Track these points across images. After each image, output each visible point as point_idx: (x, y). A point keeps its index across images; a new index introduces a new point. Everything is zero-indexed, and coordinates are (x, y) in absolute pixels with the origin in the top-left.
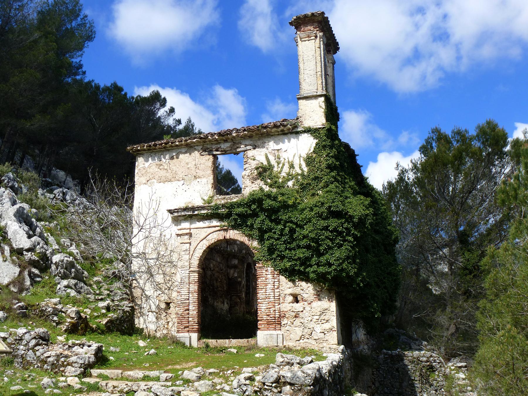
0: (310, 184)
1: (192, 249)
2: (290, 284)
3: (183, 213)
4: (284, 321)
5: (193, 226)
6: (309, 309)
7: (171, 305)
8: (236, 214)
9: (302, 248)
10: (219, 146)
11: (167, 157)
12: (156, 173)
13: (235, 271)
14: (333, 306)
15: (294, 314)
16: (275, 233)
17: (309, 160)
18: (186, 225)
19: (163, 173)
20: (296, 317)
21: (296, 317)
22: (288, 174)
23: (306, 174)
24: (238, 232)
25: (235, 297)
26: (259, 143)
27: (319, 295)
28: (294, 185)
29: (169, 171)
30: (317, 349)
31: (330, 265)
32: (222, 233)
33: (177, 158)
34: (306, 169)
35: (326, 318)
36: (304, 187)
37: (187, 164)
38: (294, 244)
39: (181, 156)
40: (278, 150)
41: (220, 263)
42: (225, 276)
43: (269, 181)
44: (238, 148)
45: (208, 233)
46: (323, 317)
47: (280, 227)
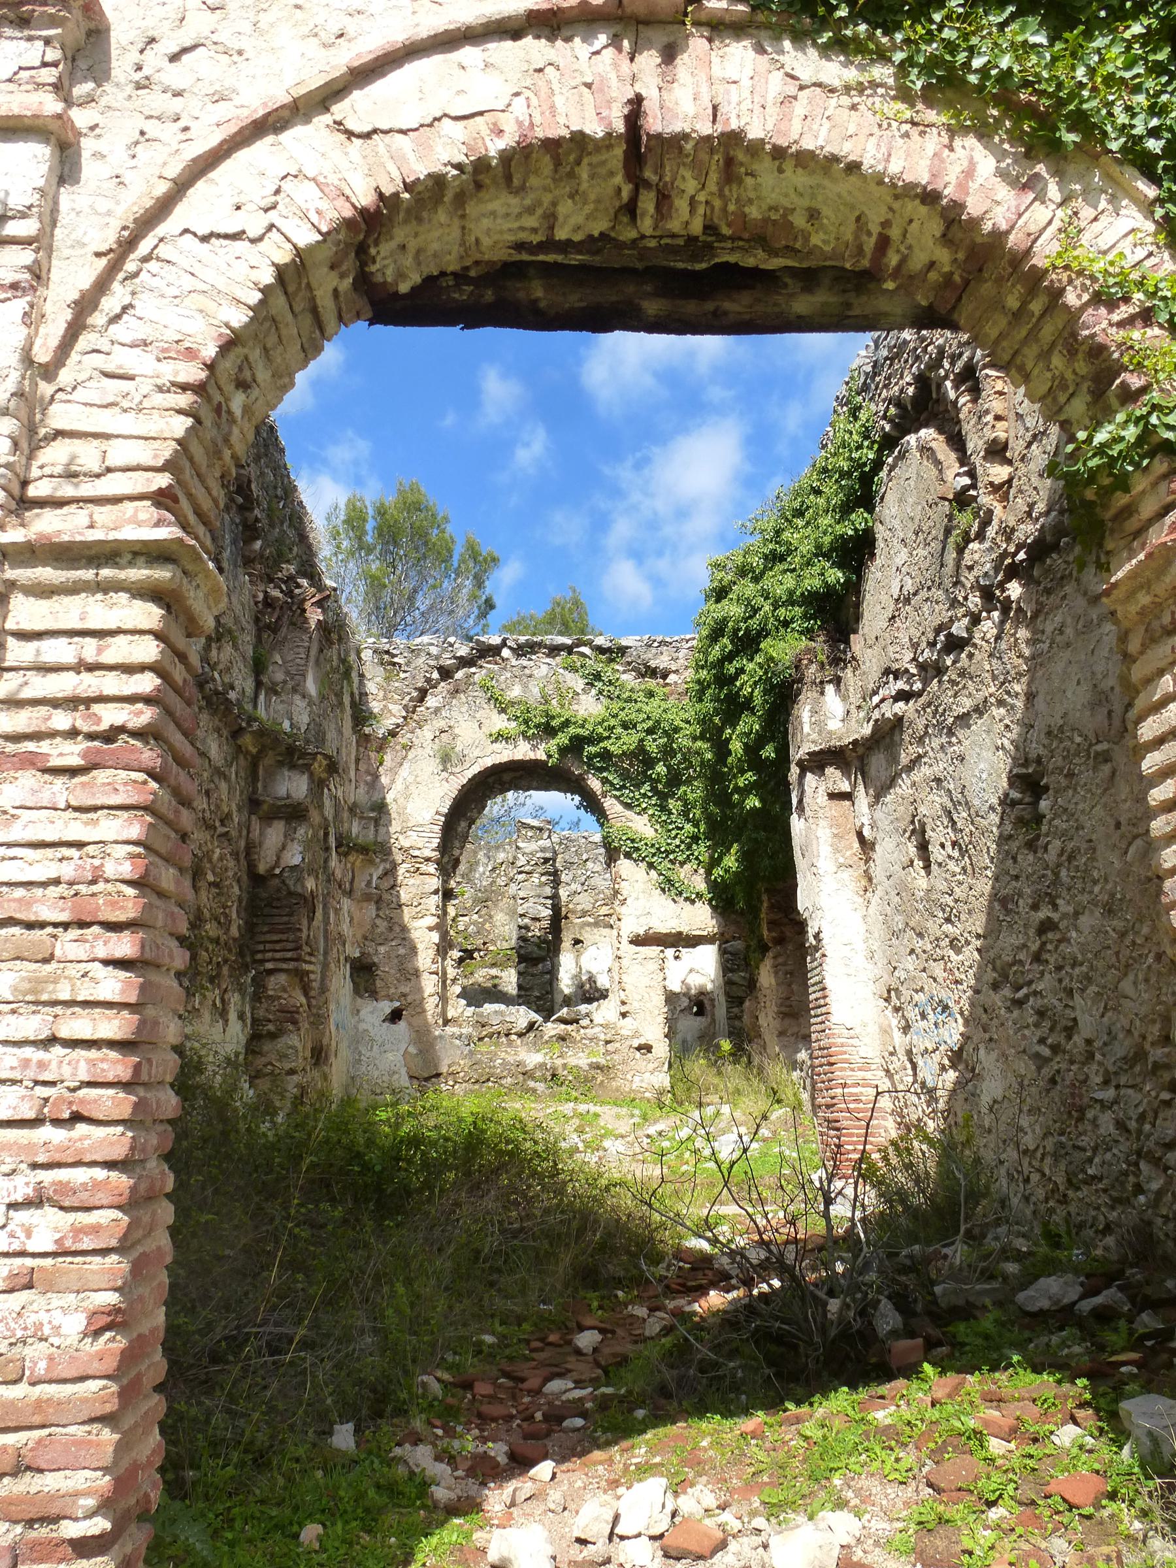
13: (289, 836)
24: (835, 71)
25: (282, 978)
41: (219, 773)
42: (235, 855)
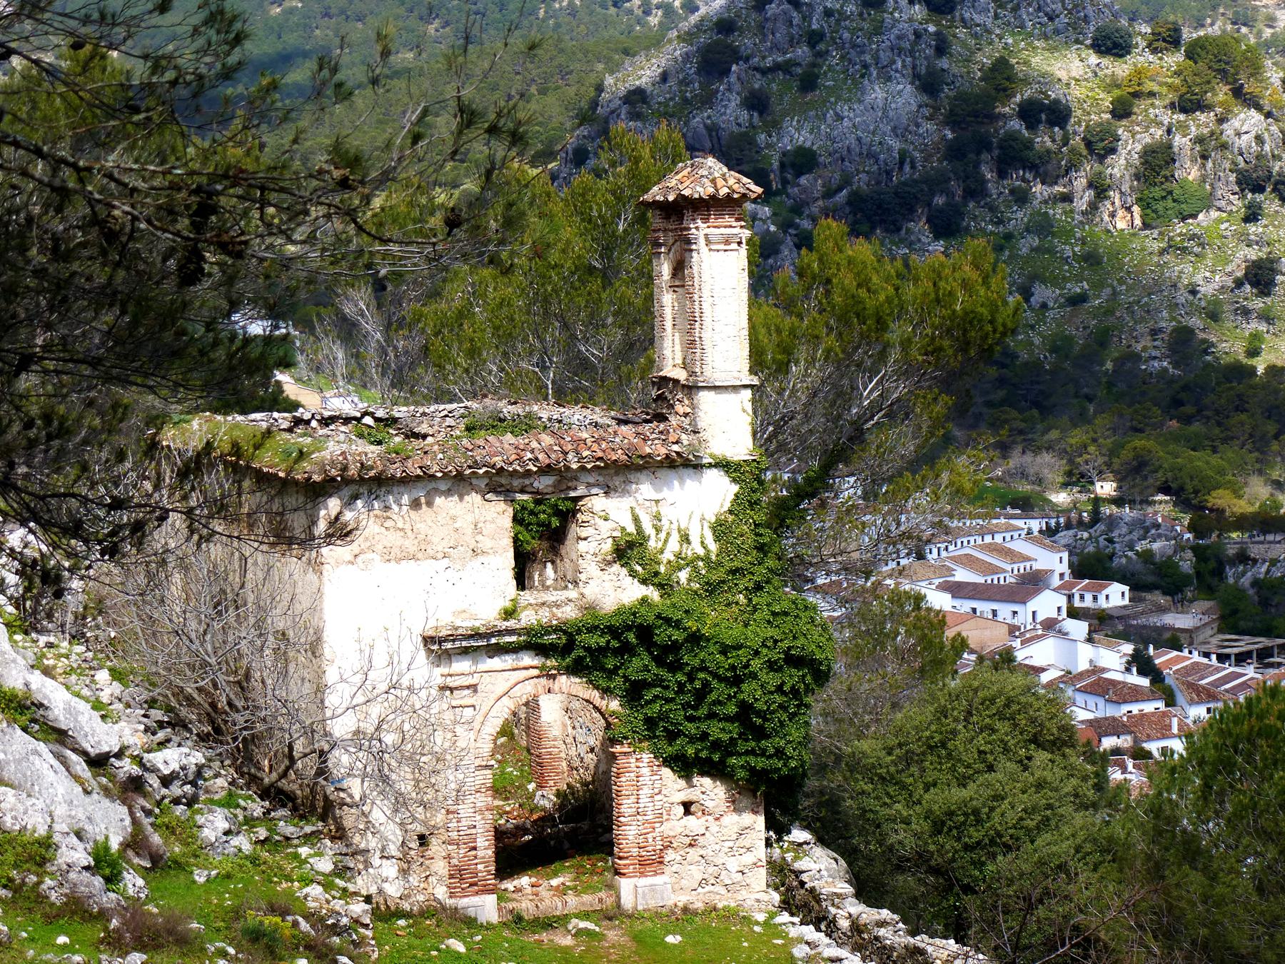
0: (723, 582)
1: (479, 719)
2: (682, 783)
3: (464, 644)
4: (670, 855)
5: (481, 667)
6: (717, 829)
7: (433, 841)
8: (588, 649)
9: (720, 720)
10: (527, 482)
11: (405, 499)
12: (377, 538)
14: (760, 821)
15: (688, 841)
16: (667, 688)
17: (720, 529)
18: (462, 665)
19: (393, 539)
20: (690, 845)
21: (690, 845)
22: (678, 556)
23: (714, 558)
24: (578, 680)
26: (617, 481)
27: (733, 802)
28: (689, 580)
29: (409, 533)
30: (733, 905)
31: (779, 753)
32: (543, 681)
33: (430, 504)
34: (713, 547)
35: (747, 844)
36: (712, 589)
37: (454, 518)
38: (703, 711)
39: (439, 501)
40: (657, 501)
43: (638, 568)
44: (569, 488)
45: (513, 681)
46: (741, 842)
47: (681, 677)
